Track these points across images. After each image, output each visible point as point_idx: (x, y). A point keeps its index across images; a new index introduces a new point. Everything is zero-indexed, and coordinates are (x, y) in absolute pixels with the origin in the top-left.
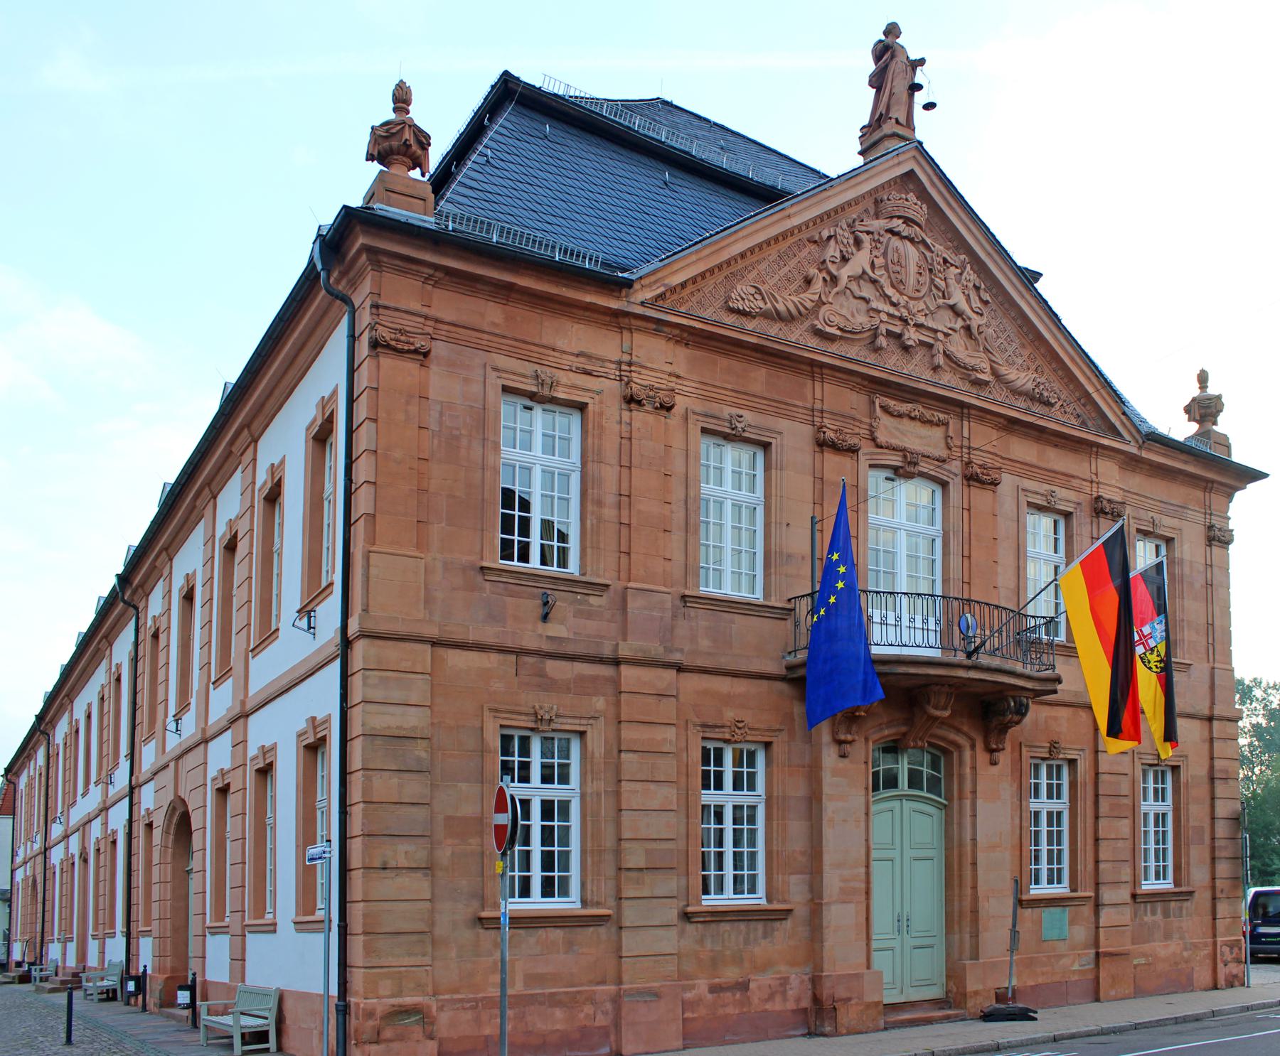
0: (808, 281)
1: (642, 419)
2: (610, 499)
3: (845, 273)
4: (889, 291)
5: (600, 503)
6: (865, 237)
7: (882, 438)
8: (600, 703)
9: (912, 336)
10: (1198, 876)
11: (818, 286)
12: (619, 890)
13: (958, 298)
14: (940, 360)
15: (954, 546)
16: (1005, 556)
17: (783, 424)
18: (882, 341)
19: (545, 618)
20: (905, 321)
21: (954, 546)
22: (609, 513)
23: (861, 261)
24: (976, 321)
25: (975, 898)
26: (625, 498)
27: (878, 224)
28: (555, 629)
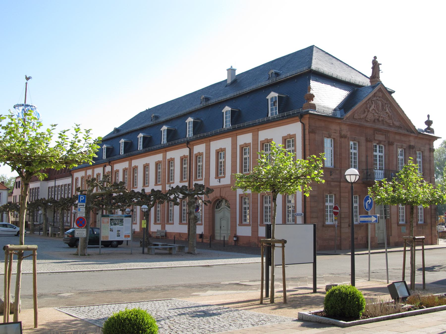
0: (365, 112)
1: (343, 139)
2: (338, 154)
3: (371, 109)
4: (377, 111)
5: (337, 155)
6: (373, 102)
7: (376, 138)
8: (338, 189)
9: (380, 119)
10: (429, 221)
11: (366, 113)
12: (340, 221)
13: (387, 111)
14: (385, 123)
15: (387, 158)
16: (395, 159)
17: (362, 138)
18: (376, 121)
19: (331, 175)
20: (379, 116)
21: (387, 158)
22: (338, 157)
23: (373, 107)
24: (390, 114)
25: (391, 224)
26: (341, 154)
27: (375, 99)
28: (332, 177)
